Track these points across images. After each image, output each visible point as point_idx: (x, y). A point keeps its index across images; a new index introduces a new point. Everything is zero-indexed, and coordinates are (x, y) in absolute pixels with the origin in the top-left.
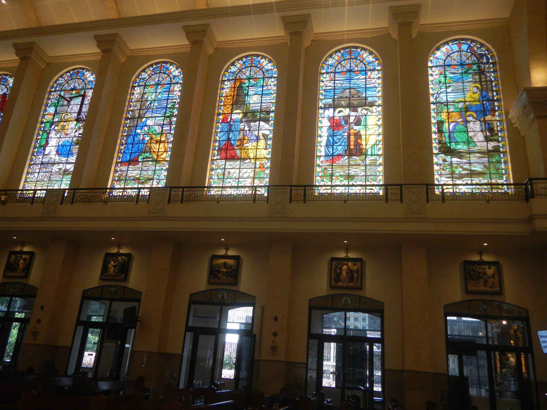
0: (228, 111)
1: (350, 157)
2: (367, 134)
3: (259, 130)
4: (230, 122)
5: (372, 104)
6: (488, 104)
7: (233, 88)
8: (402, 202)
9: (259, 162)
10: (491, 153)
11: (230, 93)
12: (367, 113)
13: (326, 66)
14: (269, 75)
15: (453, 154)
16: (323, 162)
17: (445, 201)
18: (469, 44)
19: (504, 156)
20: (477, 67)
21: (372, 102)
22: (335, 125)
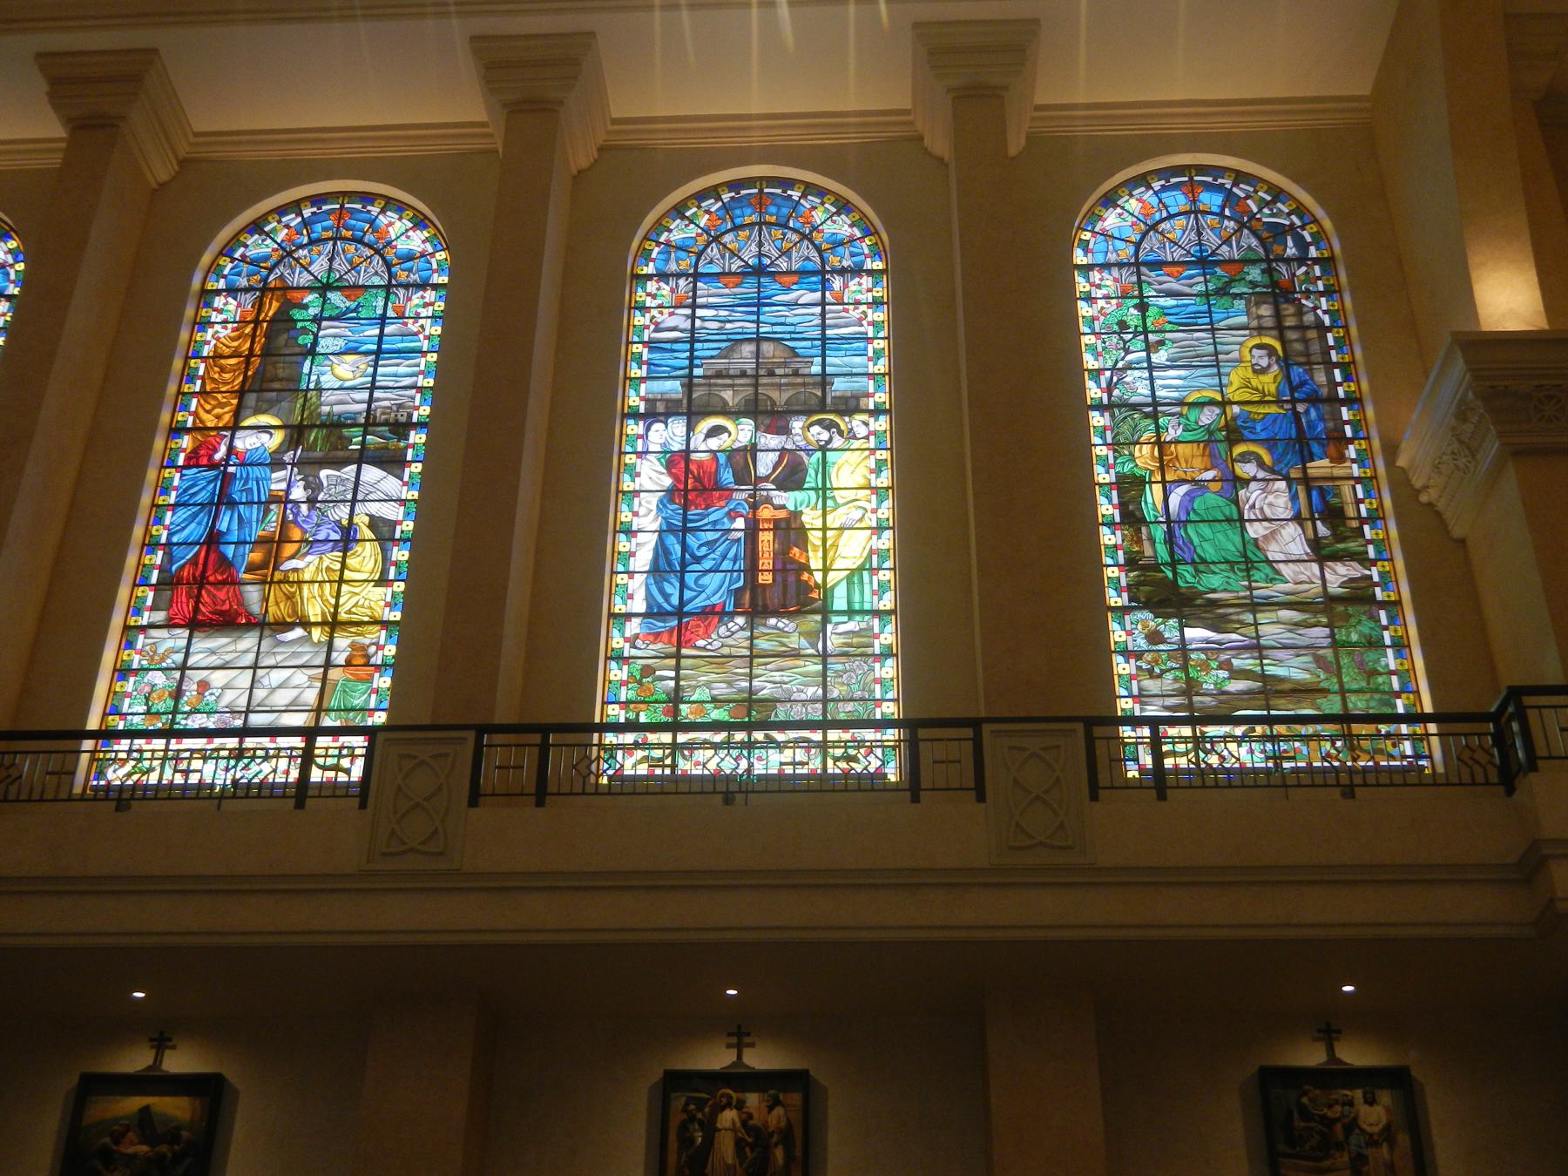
0: (218, 417)
1: (757, 620)
2: (829, 524)
3: (354, 501)
4: (227, 465)
5: (850, 406)
6: (1313, 414)
7: (250, 322)
8: (981, 798)
9: (348, 641)
10: (1341, 608)
11: (235, 344)
12: (831, 439)
13: (657, 250)
14: (414, 278)
15: (1186, 610)
16: (639, 643)
17: (1169, 792)
18: (1228, 186)
19: (1392, 619)
20: (1263, 271)
21: (849, 394)
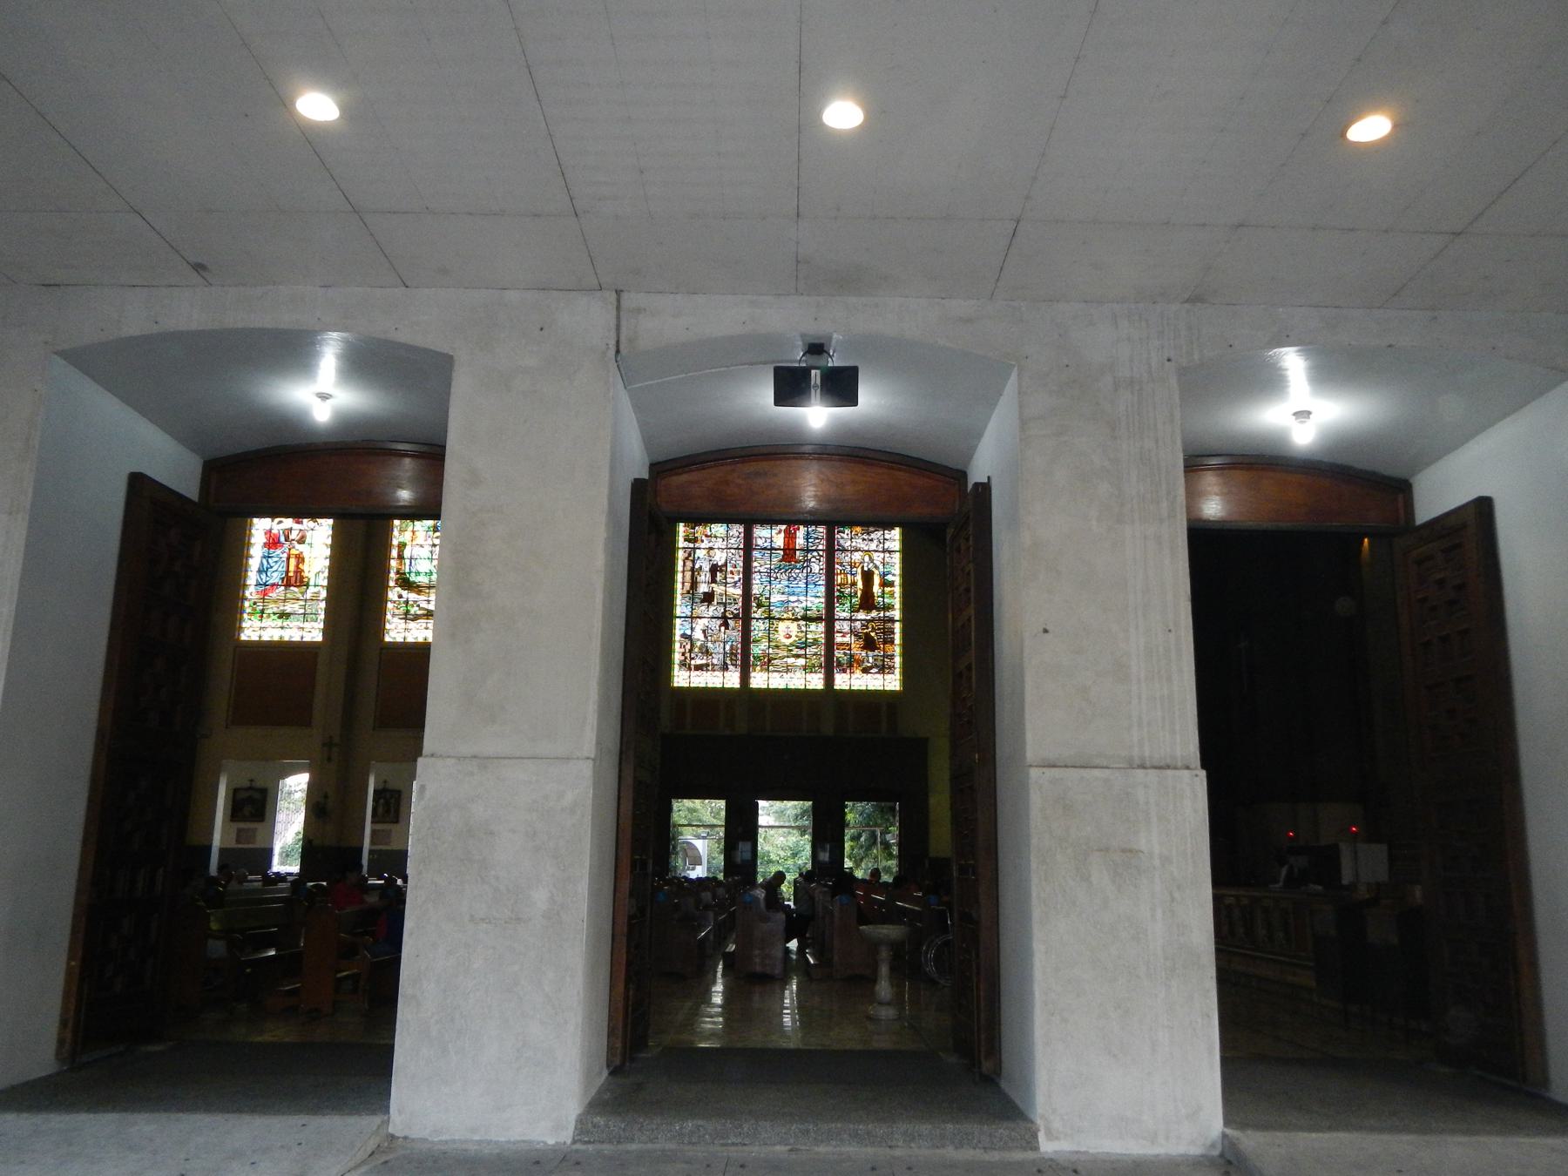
22: (273, 543)
